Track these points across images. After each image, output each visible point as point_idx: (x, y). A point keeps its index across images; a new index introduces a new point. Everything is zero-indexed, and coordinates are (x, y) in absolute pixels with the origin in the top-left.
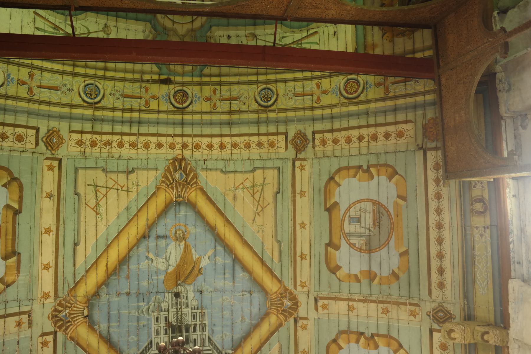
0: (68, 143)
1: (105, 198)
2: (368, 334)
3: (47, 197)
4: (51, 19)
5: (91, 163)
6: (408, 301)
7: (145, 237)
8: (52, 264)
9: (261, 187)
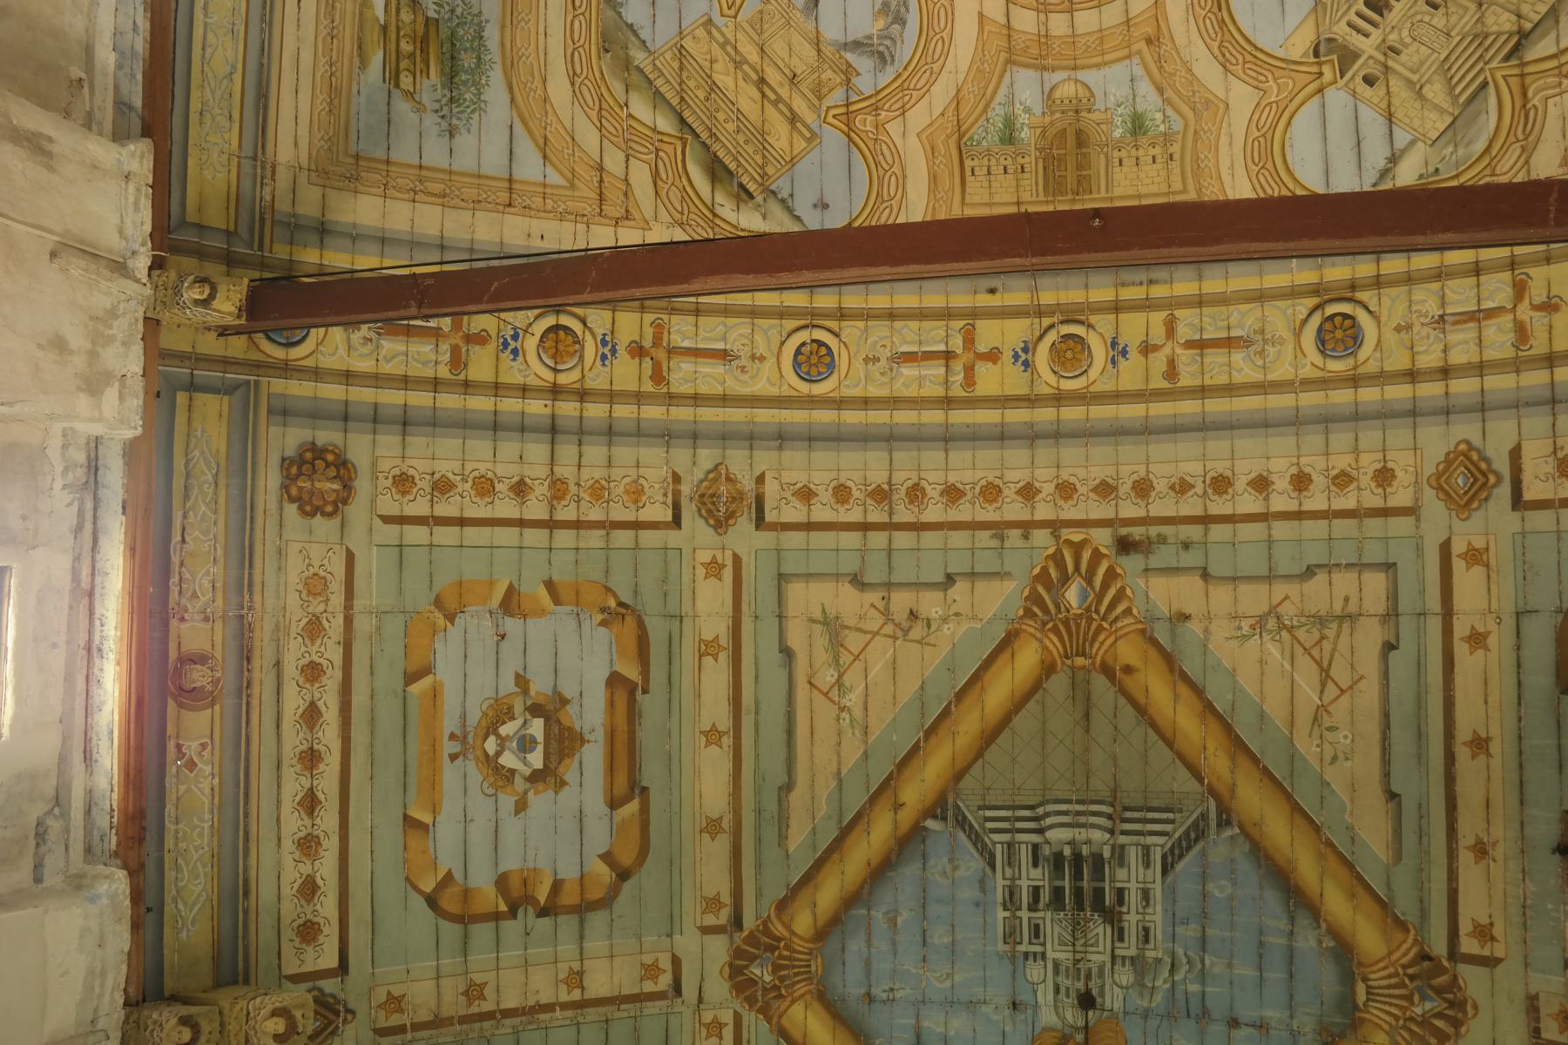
2: (527, 915)
6: (409, 1036)
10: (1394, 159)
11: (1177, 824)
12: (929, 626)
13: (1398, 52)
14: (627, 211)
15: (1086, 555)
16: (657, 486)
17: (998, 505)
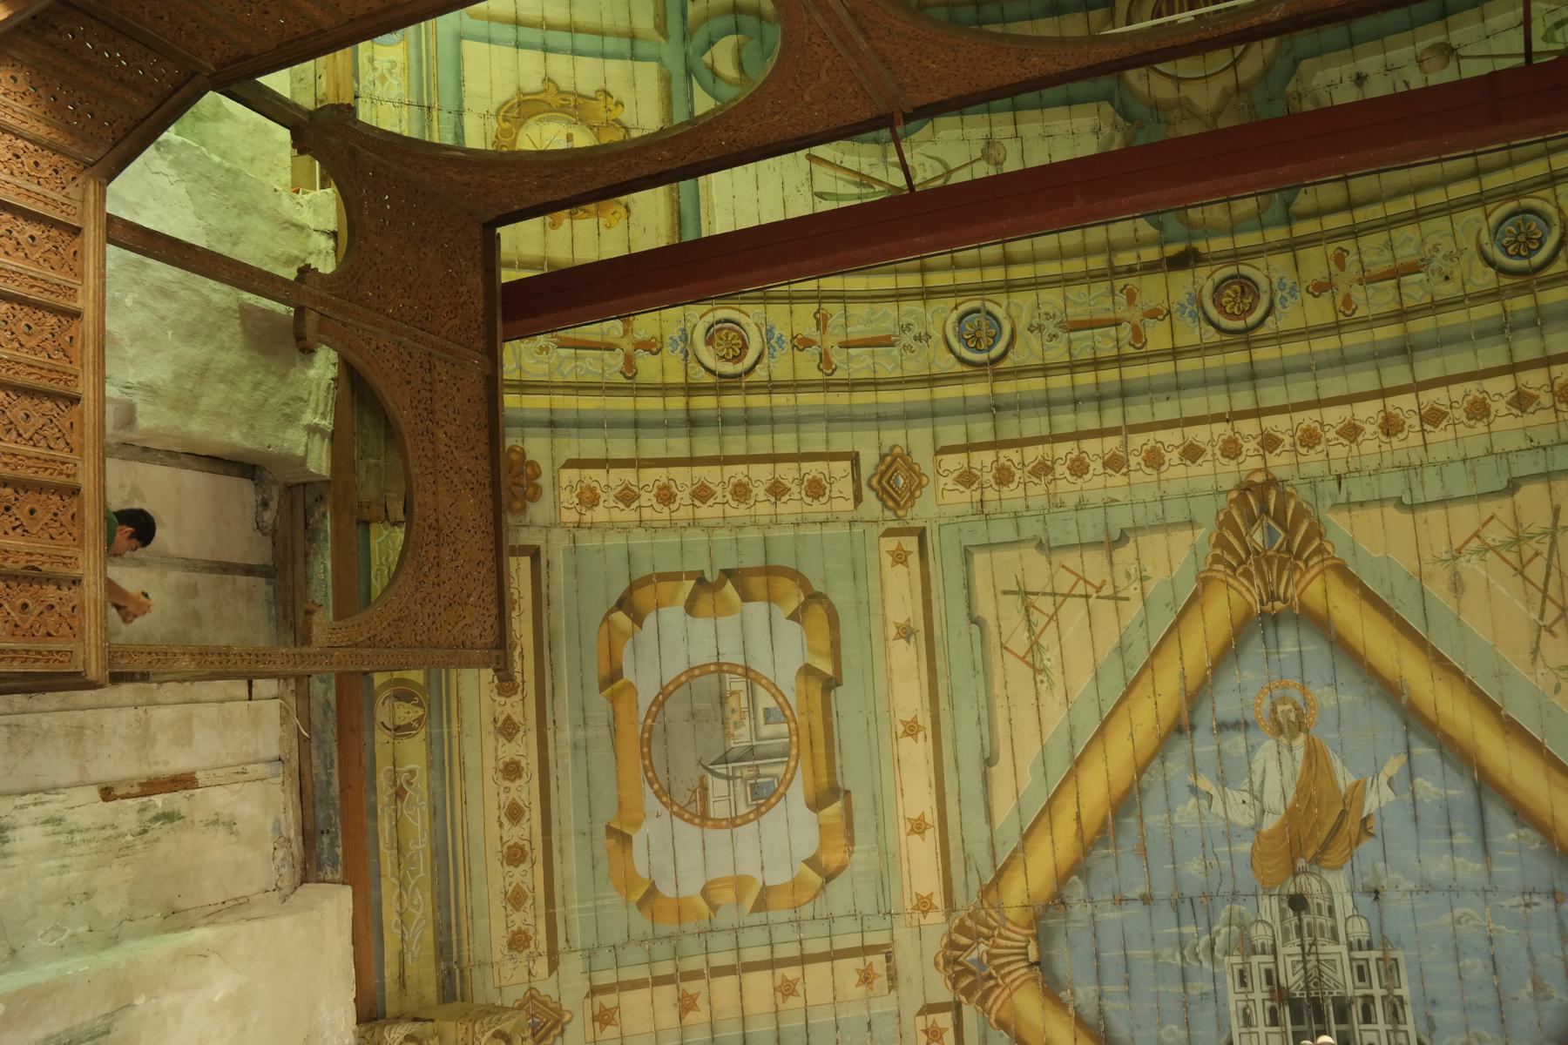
0: (936, 483)
1: (1053, 624)
3: (898, 637)
4: (850, 162)
5: (1002, 531)
7: (1181, 728)
8: (931, 818)
9: (1548, 540)
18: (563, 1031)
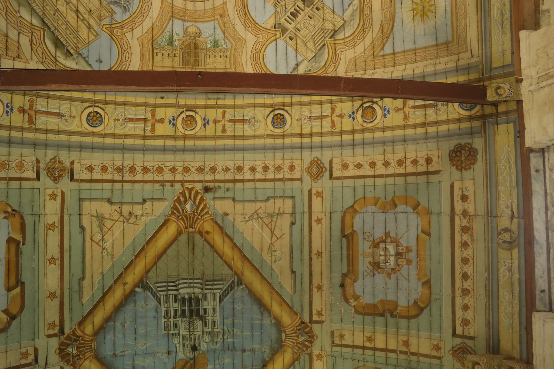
10: (297, 65)
11: (224, 286)
12: (137, 218)
13: (300, 31)
14: (19, 55)
15: (193, 193)
16: (30, 164)
17: (162, 174)
18: (453, 348)
